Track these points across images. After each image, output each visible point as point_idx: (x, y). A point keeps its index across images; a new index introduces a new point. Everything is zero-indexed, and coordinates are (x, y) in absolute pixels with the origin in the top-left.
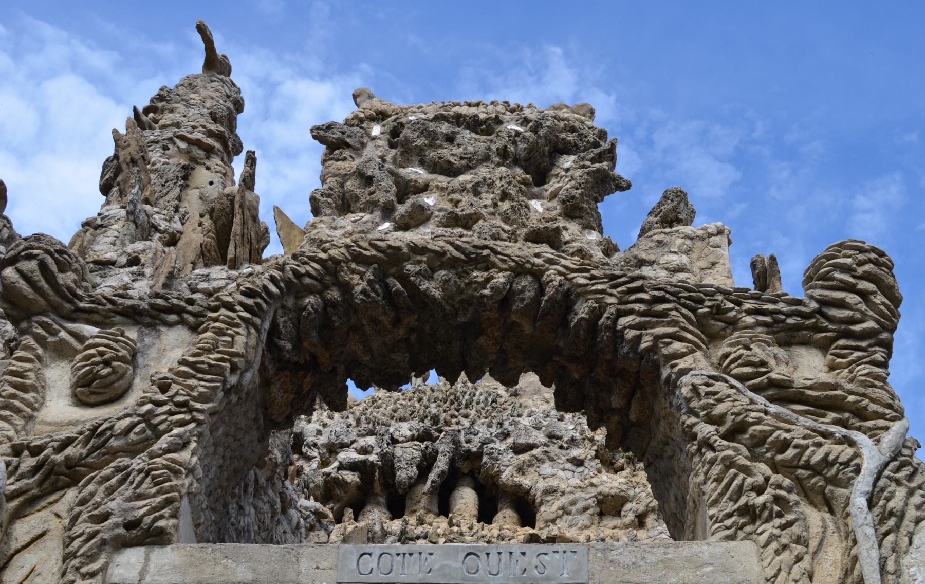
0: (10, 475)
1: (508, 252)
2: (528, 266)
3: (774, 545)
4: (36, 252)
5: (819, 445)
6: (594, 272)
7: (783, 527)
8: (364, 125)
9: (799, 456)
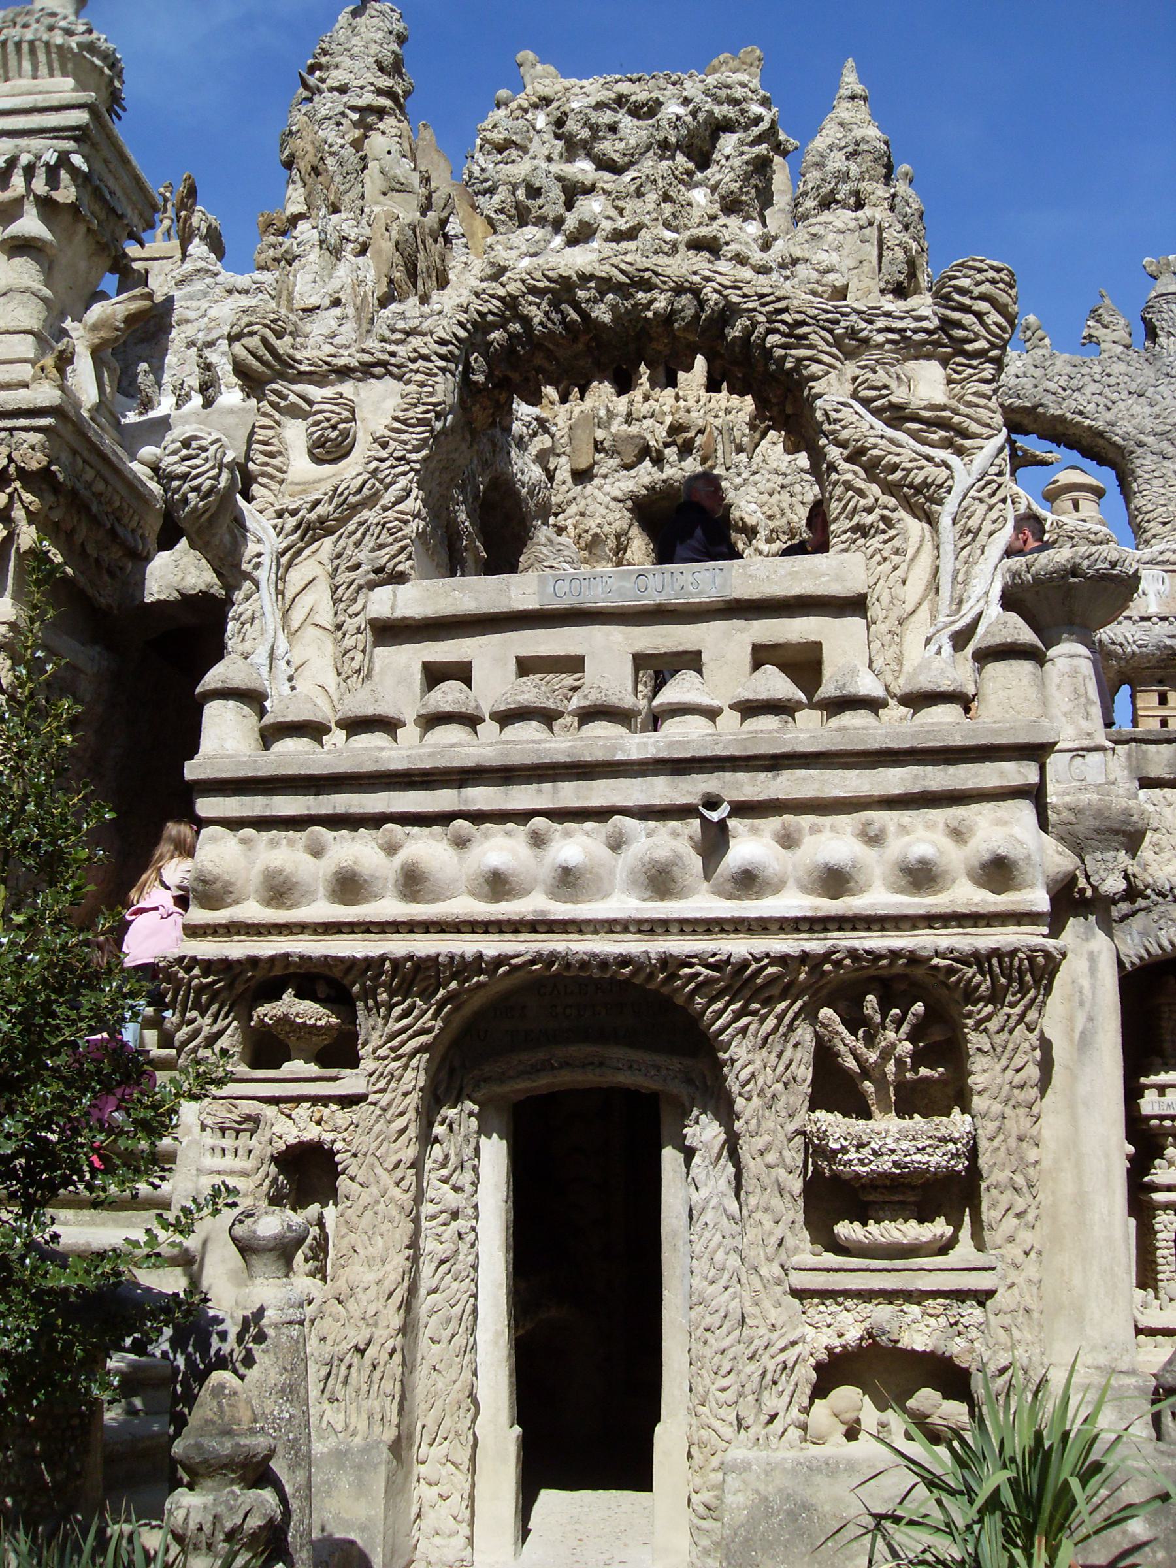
0: (278, 535)
1: (668, 272)
2: (687, 284)
3: (878, 557)
4: (255, 328)
5: (921, 468)
6: (745, 290)
7: (885, 542)
8: (529, 116)
9: (905, 477)
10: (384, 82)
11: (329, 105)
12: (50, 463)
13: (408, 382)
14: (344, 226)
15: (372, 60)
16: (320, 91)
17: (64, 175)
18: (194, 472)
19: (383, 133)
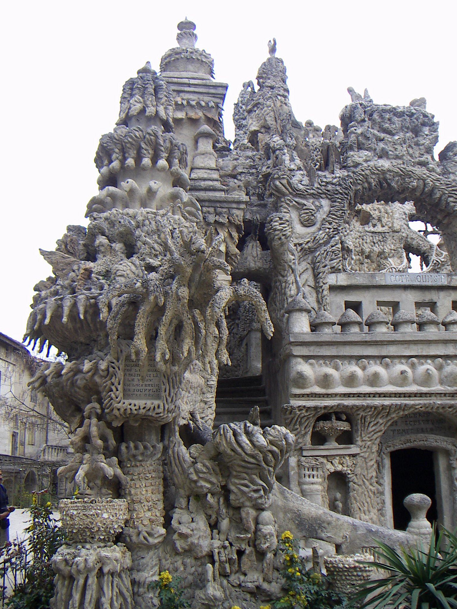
6: (441, 182)
11: (270, 93)
18: (284, 229)
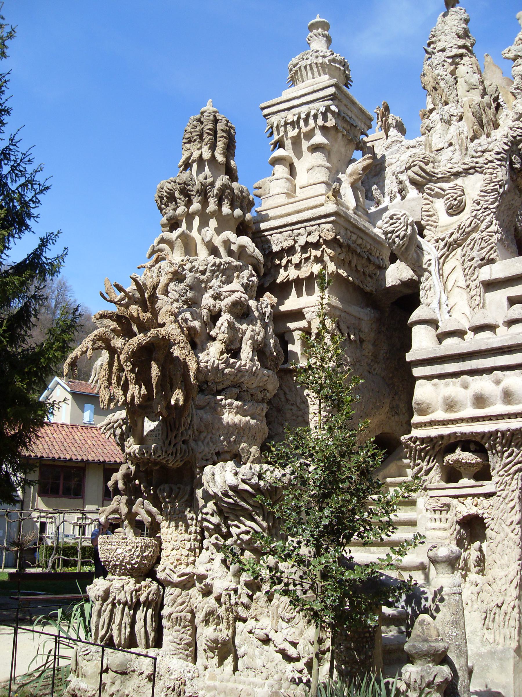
0: (437, 250)
4: (416, 163)
10: (461, 42)
11: (438, 58)
12: (336, 236)
13: (485, 174)
14: (451, 110)
15: (454, 34)
16: (434, 53)
17: (329, 115)
18: (396, 229)
19: (464, 65)
